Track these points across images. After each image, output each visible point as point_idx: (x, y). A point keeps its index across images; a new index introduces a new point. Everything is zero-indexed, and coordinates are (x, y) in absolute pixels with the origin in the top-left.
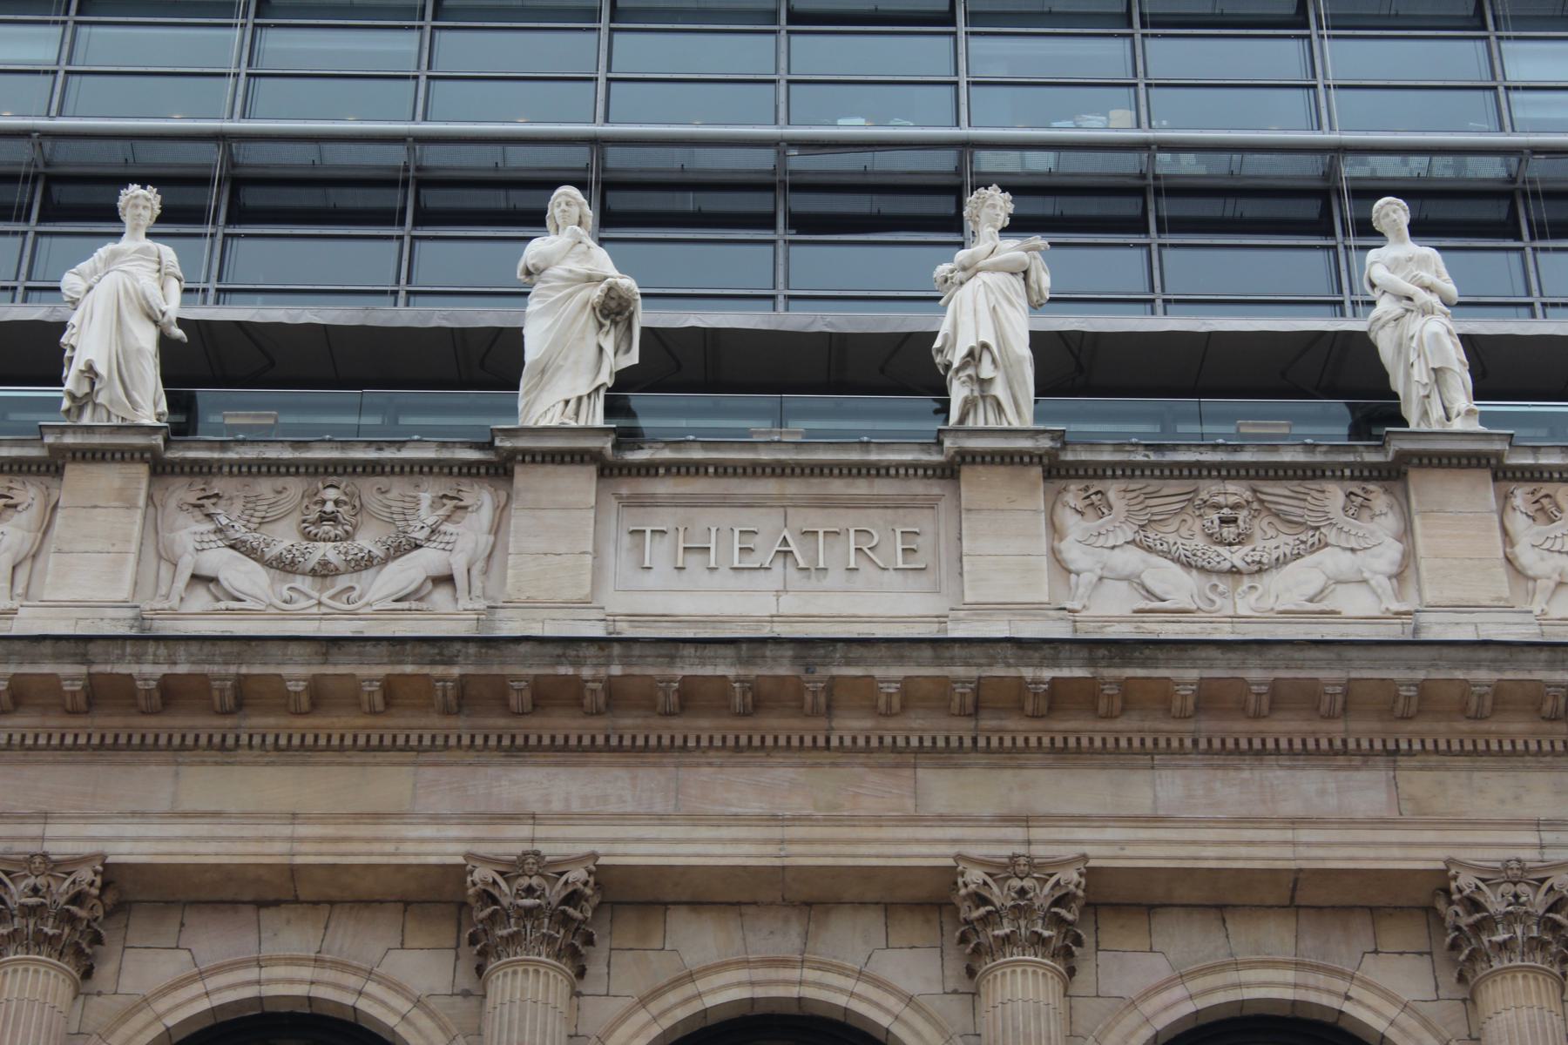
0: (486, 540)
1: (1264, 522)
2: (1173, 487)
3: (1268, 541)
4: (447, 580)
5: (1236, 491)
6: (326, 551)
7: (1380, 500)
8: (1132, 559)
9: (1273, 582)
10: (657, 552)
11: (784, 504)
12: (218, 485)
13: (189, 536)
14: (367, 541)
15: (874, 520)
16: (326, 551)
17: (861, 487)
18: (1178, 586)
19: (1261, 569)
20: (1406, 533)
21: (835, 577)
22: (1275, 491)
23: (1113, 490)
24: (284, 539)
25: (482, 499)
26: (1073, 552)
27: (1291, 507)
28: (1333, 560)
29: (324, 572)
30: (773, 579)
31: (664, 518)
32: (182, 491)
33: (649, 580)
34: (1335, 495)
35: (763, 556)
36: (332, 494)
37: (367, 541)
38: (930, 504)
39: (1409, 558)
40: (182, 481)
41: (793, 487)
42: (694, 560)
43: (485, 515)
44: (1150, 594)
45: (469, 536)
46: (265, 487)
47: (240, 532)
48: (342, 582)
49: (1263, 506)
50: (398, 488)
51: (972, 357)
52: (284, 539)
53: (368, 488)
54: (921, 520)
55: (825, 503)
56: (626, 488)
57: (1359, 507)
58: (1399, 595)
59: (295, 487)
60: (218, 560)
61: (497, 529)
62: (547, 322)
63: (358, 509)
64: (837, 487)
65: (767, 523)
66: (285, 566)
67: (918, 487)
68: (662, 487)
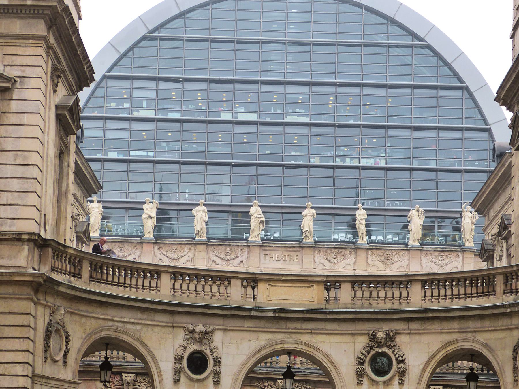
0: (247, 256)
1: (339, 255)
2: (329, 250)
3: (339, 258)
4: (242, 262)
5: (336, 251)
6: (228, 258)
7: (353, 253)
8: (323, 261)
9: (339, 264)
10: (267, 258)
11: (282, 251)
12: (215, 247)
13: (212, 254)
14: (233, 256)
15: (293, 253)
16: (228, 258)
17: (291, 249)
18: (328, 264)
19: (338, 262)
20: (355, 258)
21: (288, 261)
22: (341, 250)
23: (321, 250)
24: (223, 256)
25: (246, 249)
26: (316, 260)
27: (342, 253)
28: (346, 261)
29: (228, 260)
30: (280, 262)
31: (268, 252)
32: (210, 248)
33: (266, 262)
34: (348, 251)
35: (280, 259)
36: (228, 249)
37: (233, 256)
38: (300, 251)
39: (356, 261)
40: (210, 246)
41: (283, 249)
42: (271, 259)
43: (246, 253)
44: (325, 266)
45: (245, 255)
46: (220, 247)
47: (218, 255)
48: (230, 262)
49: (339, 253)
50: (236, 248)
51: (306, 231)
52: (223, 256)
53: (232, 248)
54: (299, 253)
55: (287, 251)
56: (263, 248)
57: (350, 253)
58: (354, 267)
59: (224, 247)
60: (216, 258)
61: (248, 255)
62: (253, 224)
63: (231, 251)
64: (288, 249)
65: (280, 253)
66: (223, 259)
67: (298, 249)
68: (267, 248)
